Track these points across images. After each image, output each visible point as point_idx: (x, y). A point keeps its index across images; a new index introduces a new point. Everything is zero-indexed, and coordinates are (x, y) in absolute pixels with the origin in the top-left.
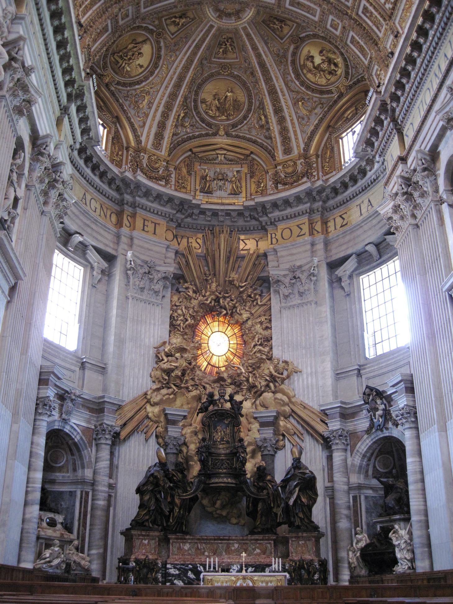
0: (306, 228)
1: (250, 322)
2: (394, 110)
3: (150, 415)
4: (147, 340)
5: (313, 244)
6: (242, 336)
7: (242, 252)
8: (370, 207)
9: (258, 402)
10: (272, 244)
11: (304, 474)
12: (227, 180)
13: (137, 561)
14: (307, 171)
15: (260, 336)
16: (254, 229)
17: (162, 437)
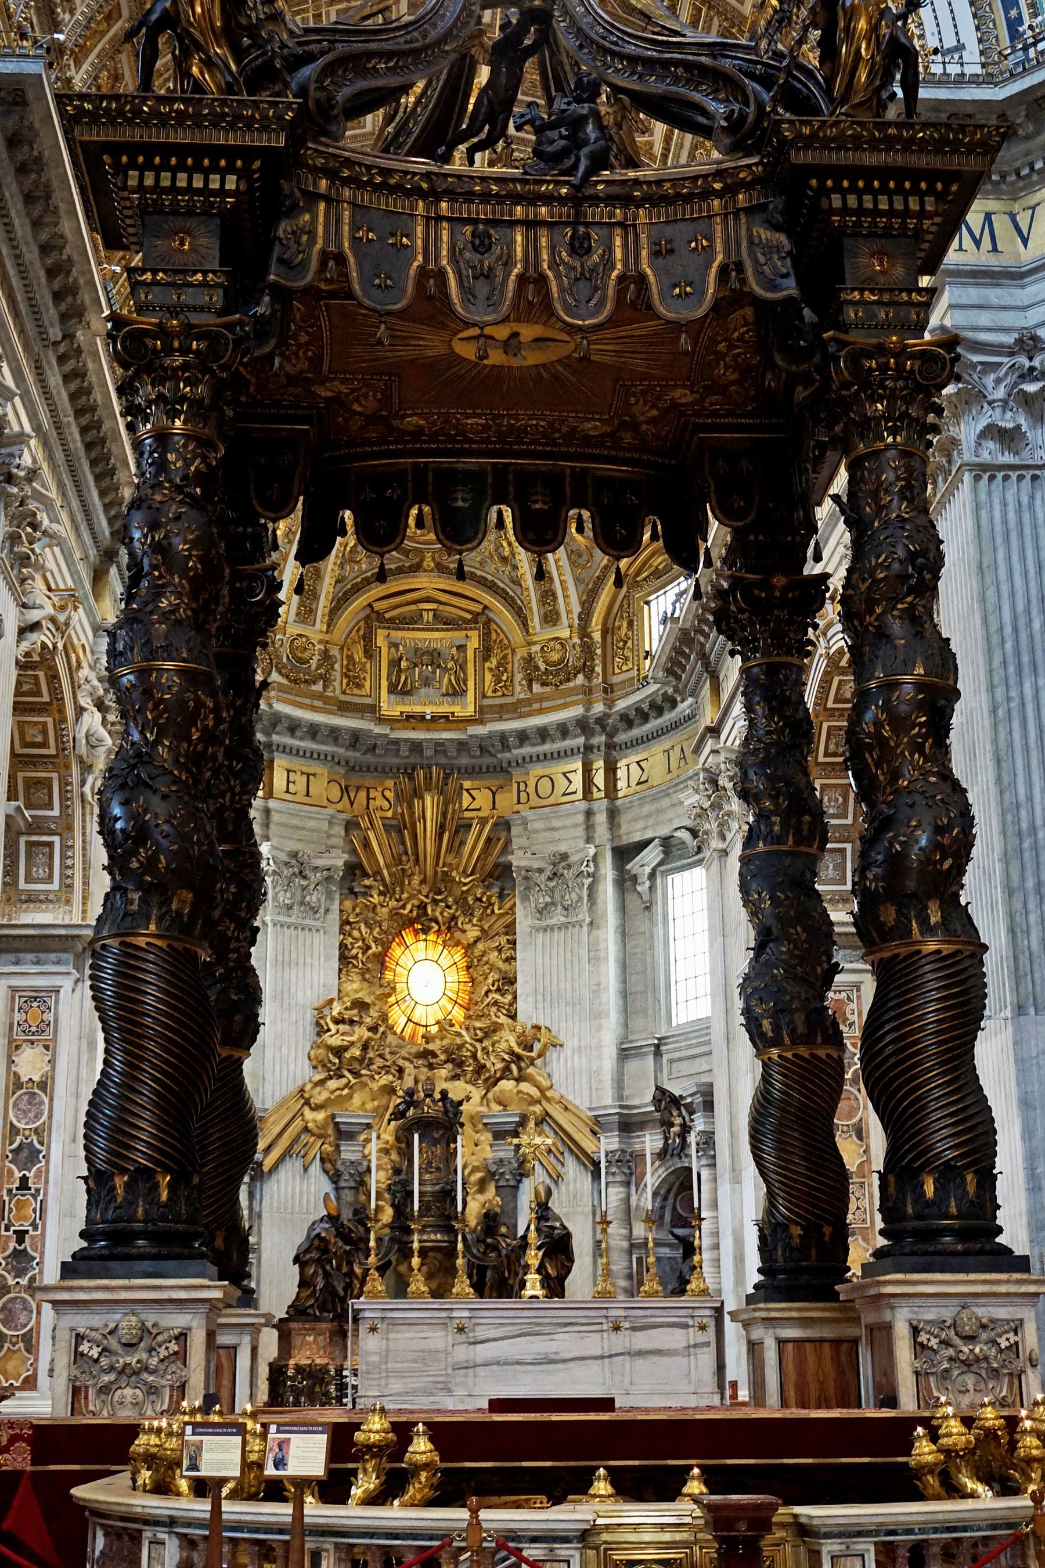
0: (577, 779)
1: (480, 946)
2: (702, 645)
3: (310, 1125)
4: (300, 995)
5: (589, 814)
6: (468, 968)
7: (467, 814)
8: (683, 762)
9: (490, 1095)
10: (519, 802)
11: (553, 1228)
12: (439, 666)
13: (299, 1369)
14: (585, 664)
15: (496, 977)
16: (488, 771)
17: (330, 1161)
